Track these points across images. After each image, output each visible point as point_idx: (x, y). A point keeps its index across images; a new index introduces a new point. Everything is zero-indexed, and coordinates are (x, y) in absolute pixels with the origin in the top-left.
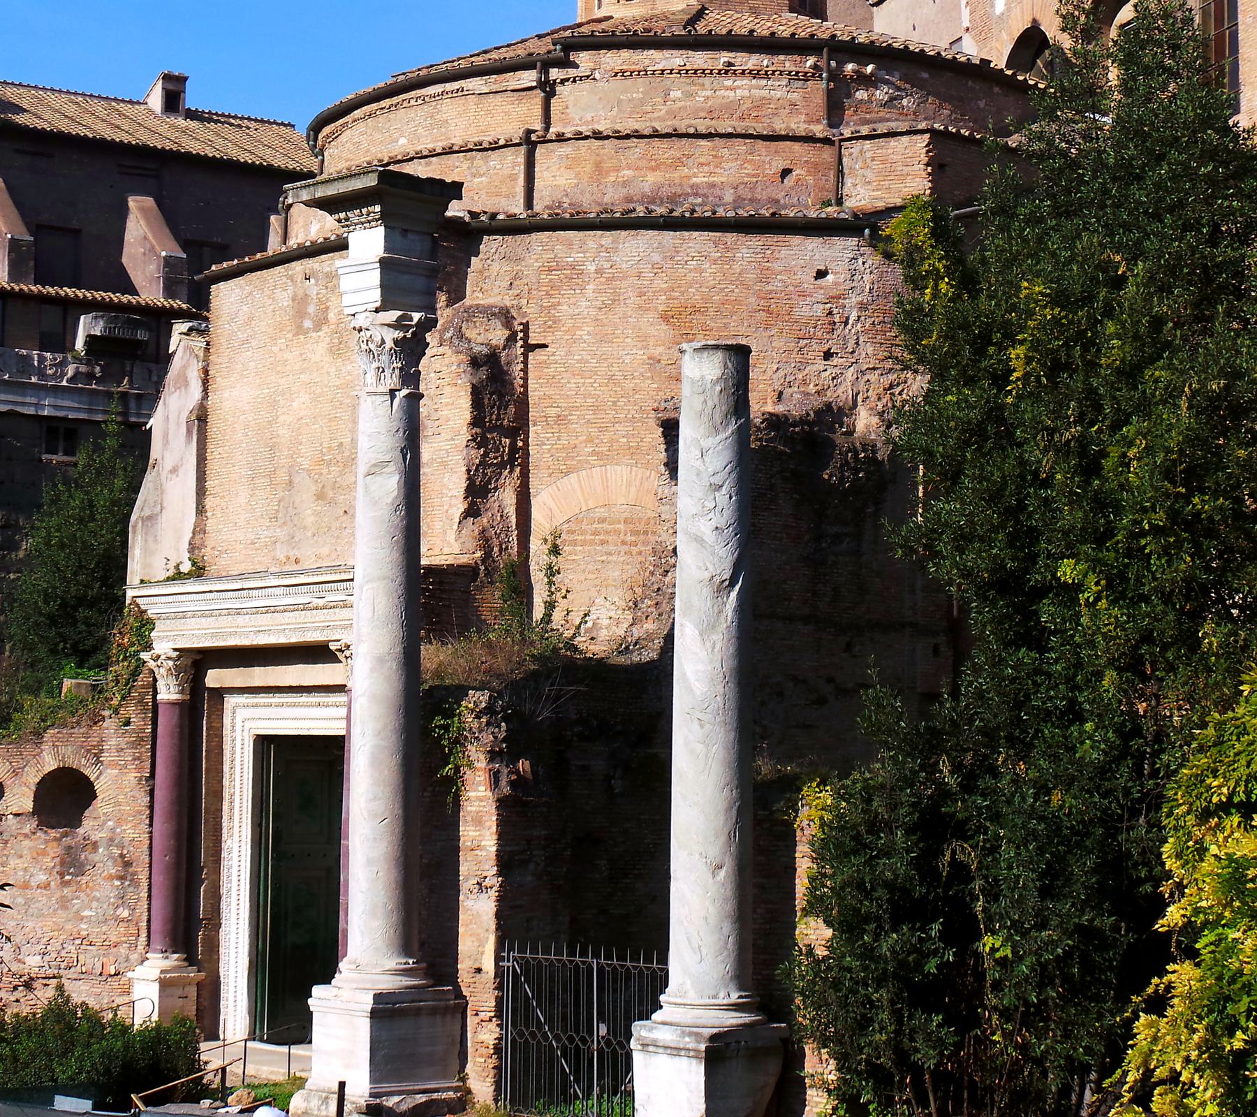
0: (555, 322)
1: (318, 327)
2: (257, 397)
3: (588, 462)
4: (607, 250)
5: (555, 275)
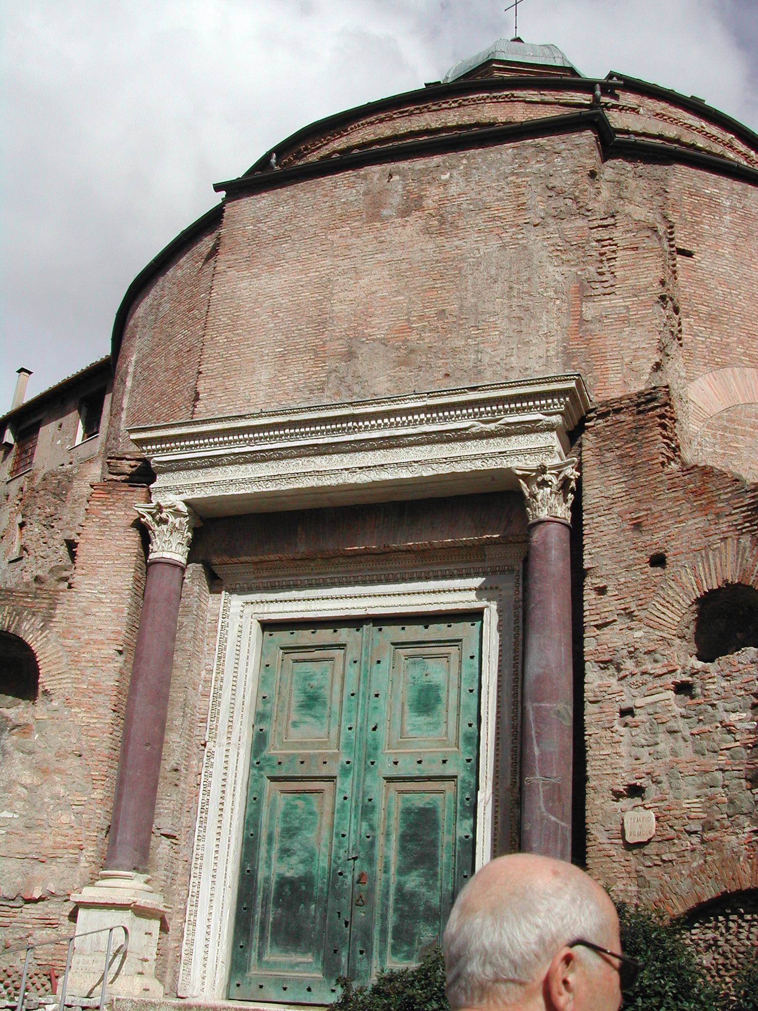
0: (698, 236)
1: (405, 213)
2: (298, 280)
3: (741, 361)
4: (738, 194)
5: (695, 200)
